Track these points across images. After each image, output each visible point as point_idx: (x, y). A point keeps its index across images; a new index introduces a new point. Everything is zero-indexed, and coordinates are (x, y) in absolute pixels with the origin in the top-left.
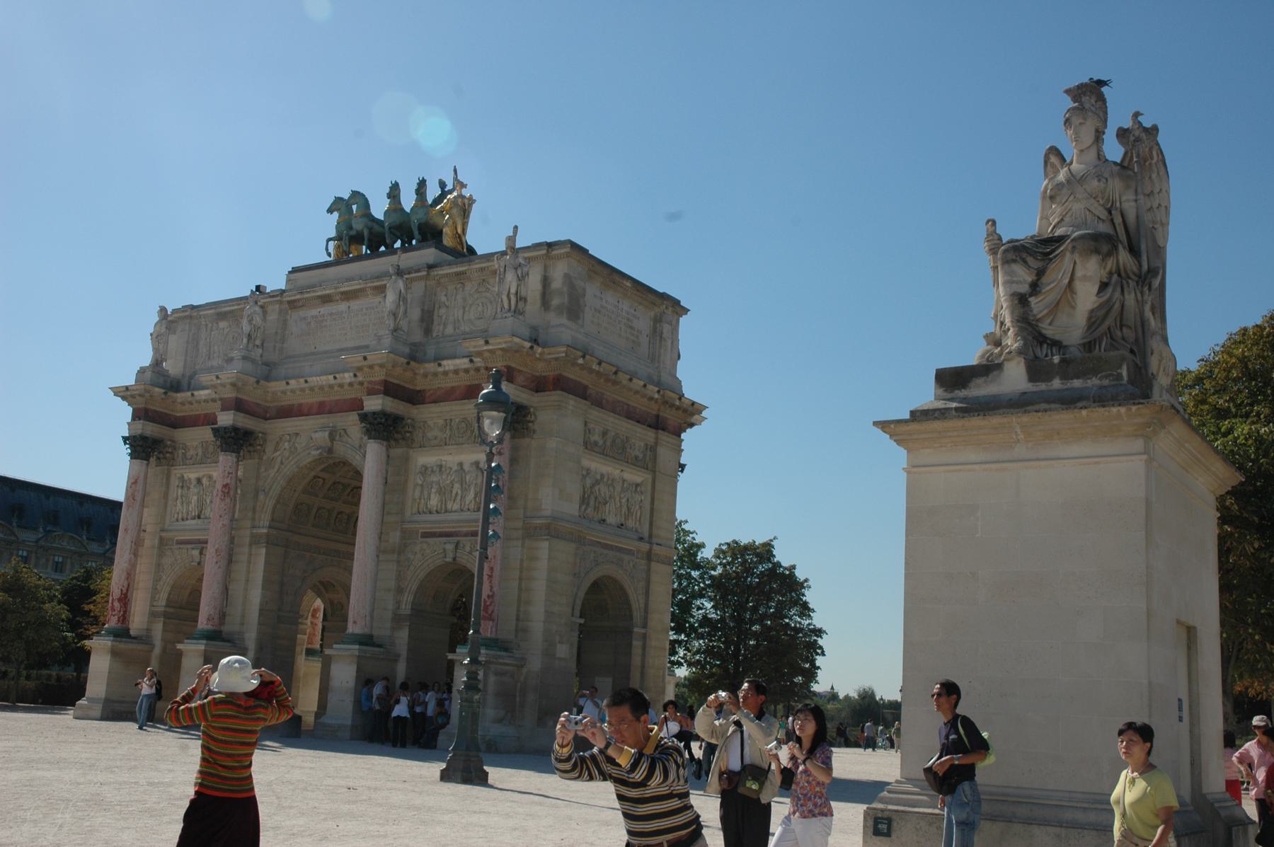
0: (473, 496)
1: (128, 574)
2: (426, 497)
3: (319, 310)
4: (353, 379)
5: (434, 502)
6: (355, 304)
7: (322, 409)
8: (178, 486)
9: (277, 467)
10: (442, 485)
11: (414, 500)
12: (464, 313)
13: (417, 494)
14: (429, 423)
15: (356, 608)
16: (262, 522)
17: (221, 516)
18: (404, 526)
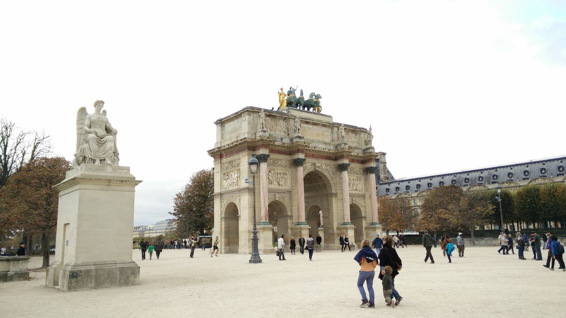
3: (303, 125)
4: (328, 151)
6: (315, 127)
7: (313, 156)
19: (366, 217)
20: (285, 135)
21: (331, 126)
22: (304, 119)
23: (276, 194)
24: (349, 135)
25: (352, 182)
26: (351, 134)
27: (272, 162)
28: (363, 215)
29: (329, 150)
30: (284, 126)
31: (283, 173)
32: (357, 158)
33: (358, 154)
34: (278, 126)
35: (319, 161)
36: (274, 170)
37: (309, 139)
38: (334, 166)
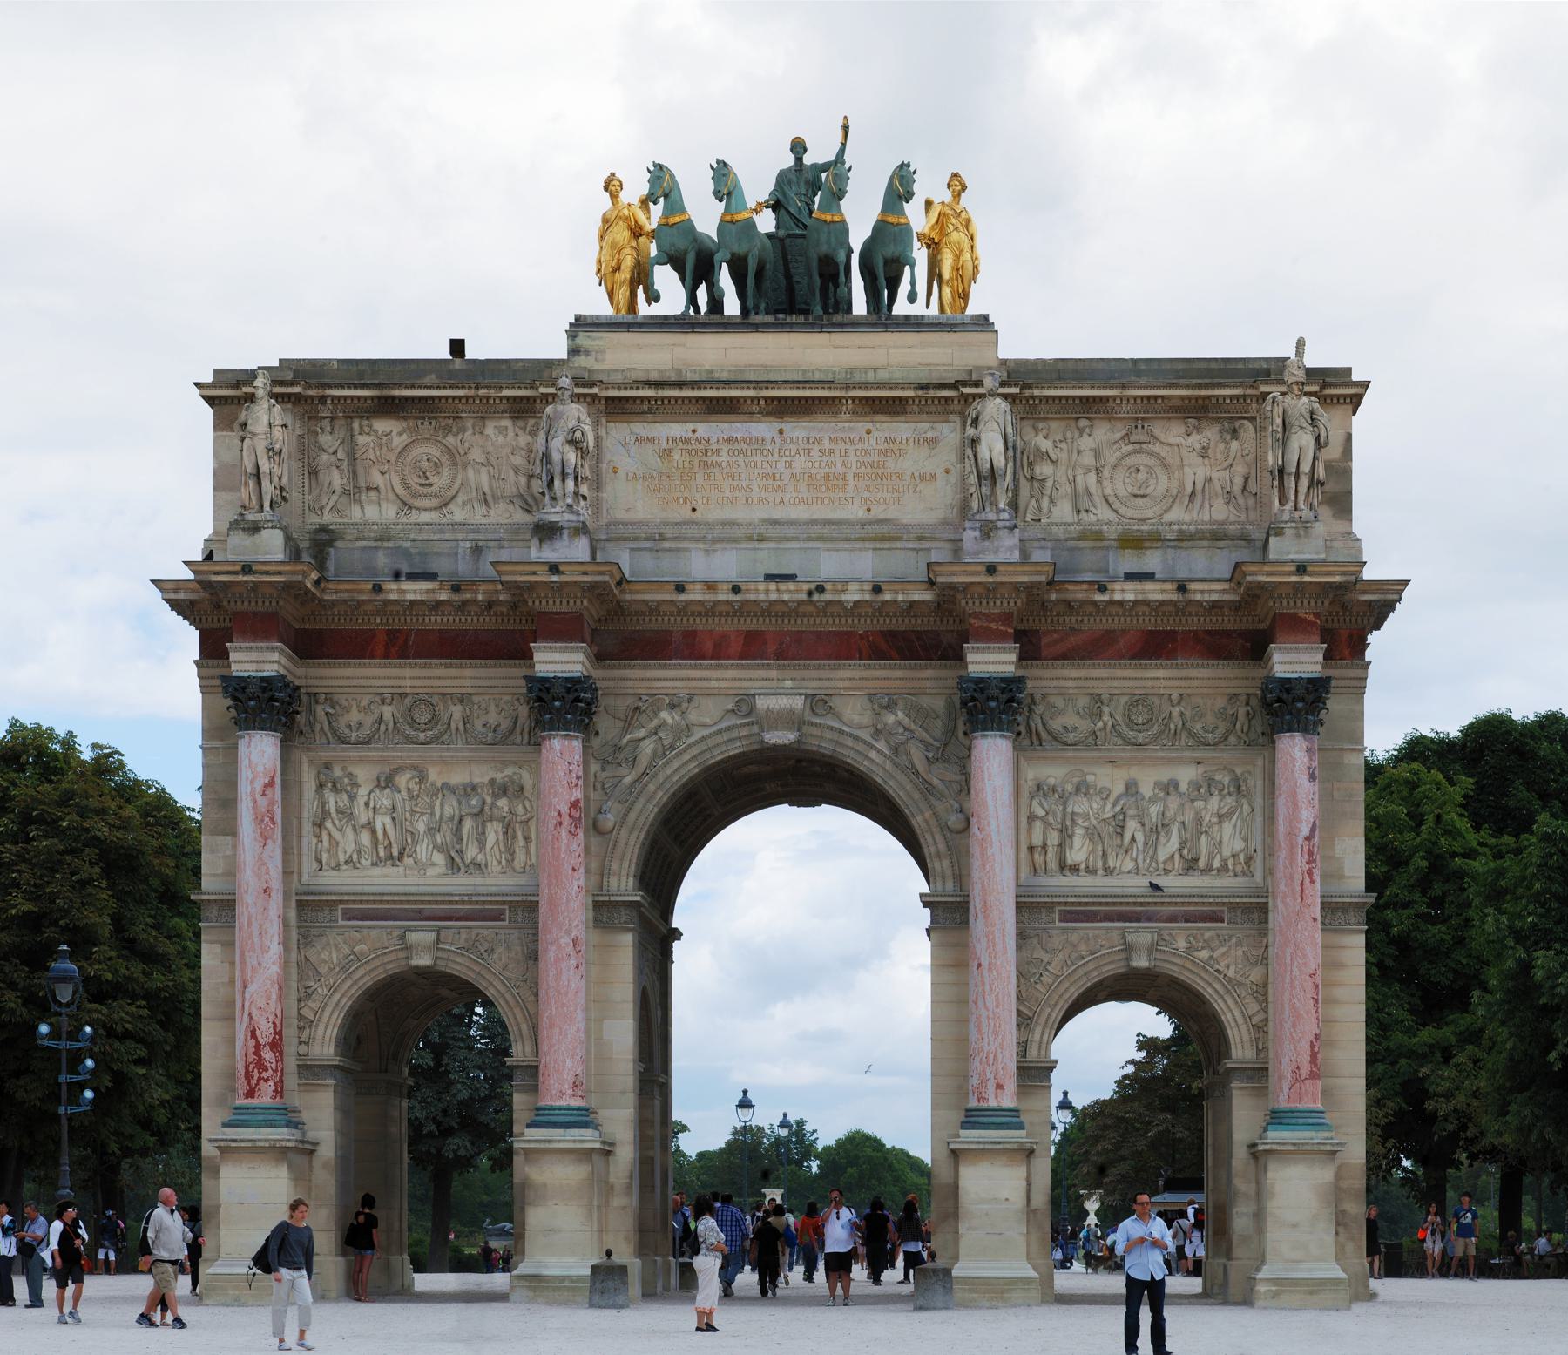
0: (1177, 846)
1: (280, 988)
2: (1056, 842)
3: (691, 426)
4: (868, 597)
5: (1078, 853)
6: (797, 429)
7: (752, 647)
8: (321, 786)
9: (643, 762)
10: (1094, 822)
11: (1031, 849)
12: (1100, 482)
13: (1037, 840)
14: (1052, 699)
15: (1000, 1056)
16: (614, 883)
17: (574, 870)
18: (1023, 899)
19: (1267, 1069)
20: (527, 518)
21: (946, 399)
22: (694, 385)
23: (409, 929)
24: (1157, 448)
25: (1154, 810)
26: (1173, 435)
27: (387, 716)
28: (1241, 1051)
29: (877, 589)
30: (518, 460)
31: (492, 781)
32: (1196, 623)
33: (1182, 588)
34: (465, 467)
35: (814, 674)
36: (413, 767)
37: (733, 524)
38: (957, 700)
